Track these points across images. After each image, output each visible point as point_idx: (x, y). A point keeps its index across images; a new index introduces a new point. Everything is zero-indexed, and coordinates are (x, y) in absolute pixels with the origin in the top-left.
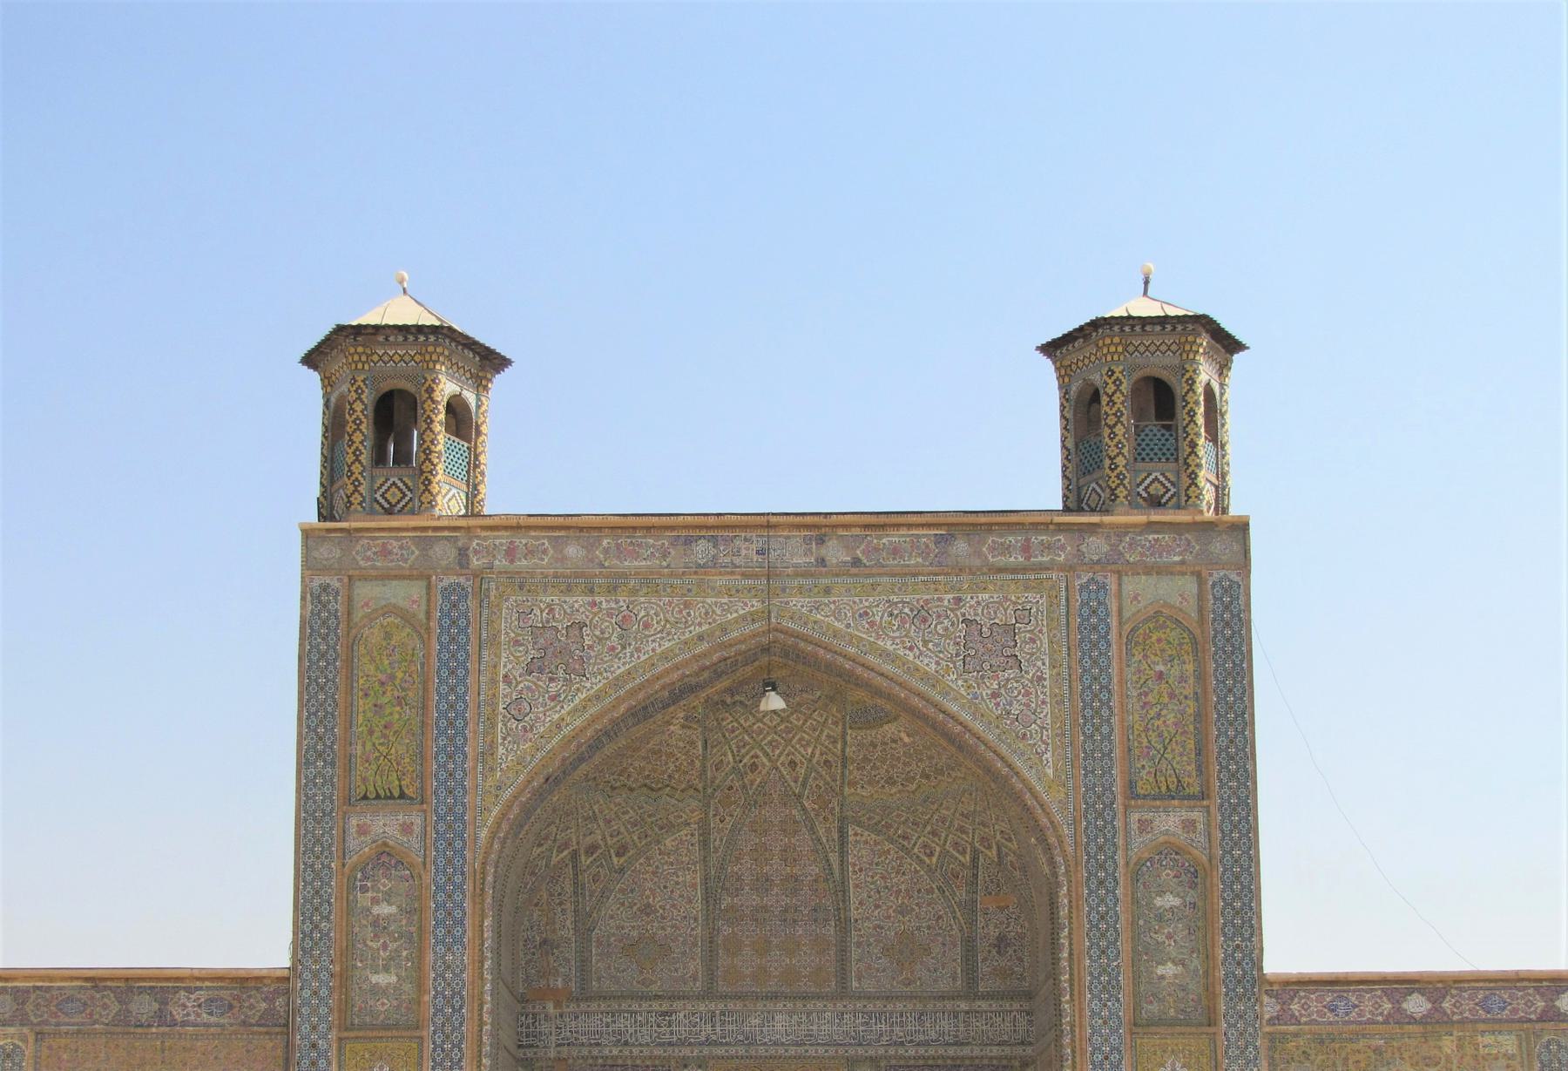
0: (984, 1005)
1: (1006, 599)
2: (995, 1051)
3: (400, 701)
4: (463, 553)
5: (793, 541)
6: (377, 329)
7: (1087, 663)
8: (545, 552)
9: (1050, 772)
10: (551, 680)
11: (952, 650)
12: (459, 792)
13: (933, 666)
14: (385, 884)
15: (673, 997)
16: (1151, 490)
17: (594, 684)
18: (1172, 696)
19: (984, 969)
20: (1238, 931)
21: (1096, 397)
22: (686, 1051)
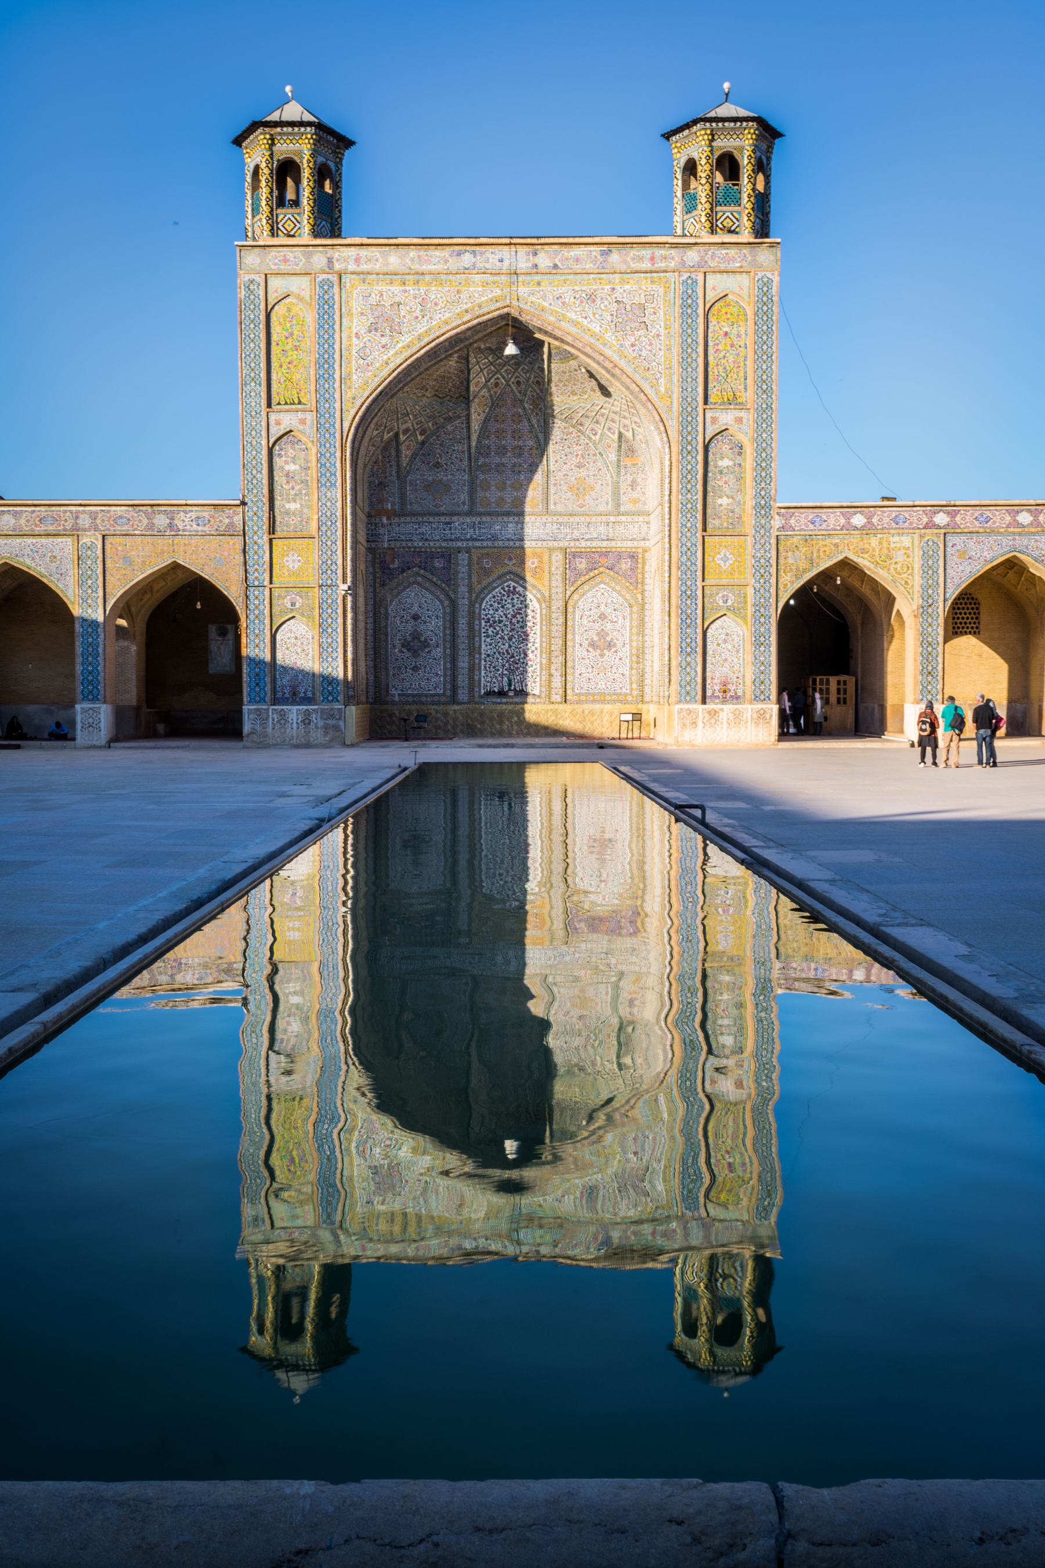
0: (623, 518)
1: (640, 288)
2: (629, 544)
3: (296, 348)
4: (330, 261)
9: (662, 389)
11: (609, 318)
13: (598, 328)
14: (291, 452)
16: (725, 223)
17: (406, 339)
18: (732, 346)
20: (763, 480)
22: (459, 544)
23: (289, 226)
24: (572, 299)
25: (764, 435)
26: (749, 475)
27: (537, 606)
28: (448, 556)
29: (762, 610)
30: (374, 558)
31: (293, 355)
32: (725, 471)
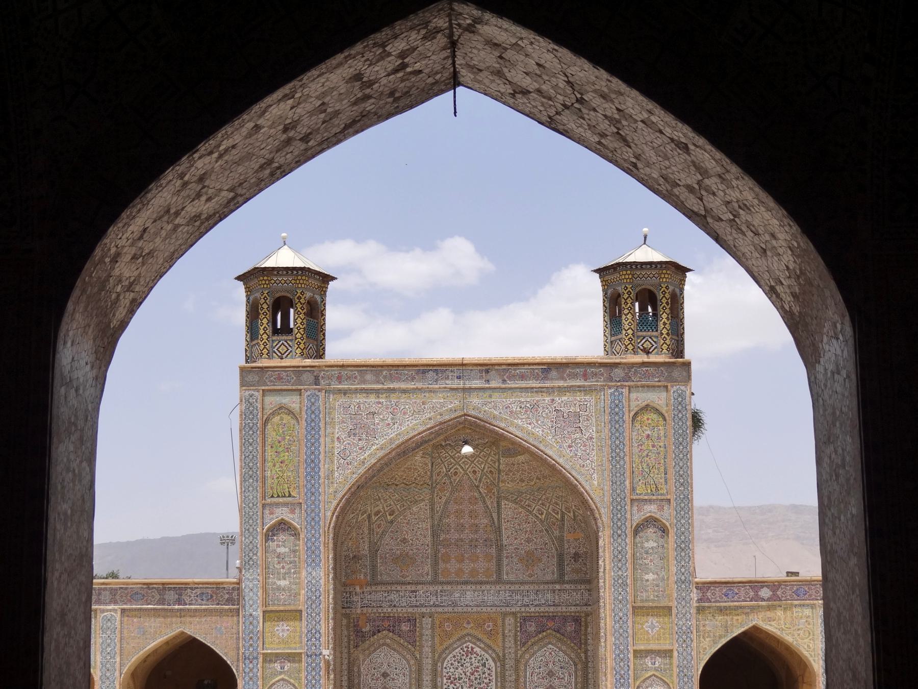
0: (567, 586)
2: (573, 609)
5: (473, 372)
6: (273, 268)
7: (614, 430)
8: (356, 378)
9: (596, 483)
10: (360, 440)
12: (317, 494)
15: (417, 583)
17: (381, 441)
18: (653, 446)
19: (568, 569)
20: (682, 558)
21: (619, 295)
22: (424, 610)
23: (283, 349)
24: (518, 409)
25: (683, 521)
26: (672, 554)
27: (493, 664)
28: (412, 620)
29: (685, 670)
30: (349, 622)
31: (285, 456)
32: (651, 551)
